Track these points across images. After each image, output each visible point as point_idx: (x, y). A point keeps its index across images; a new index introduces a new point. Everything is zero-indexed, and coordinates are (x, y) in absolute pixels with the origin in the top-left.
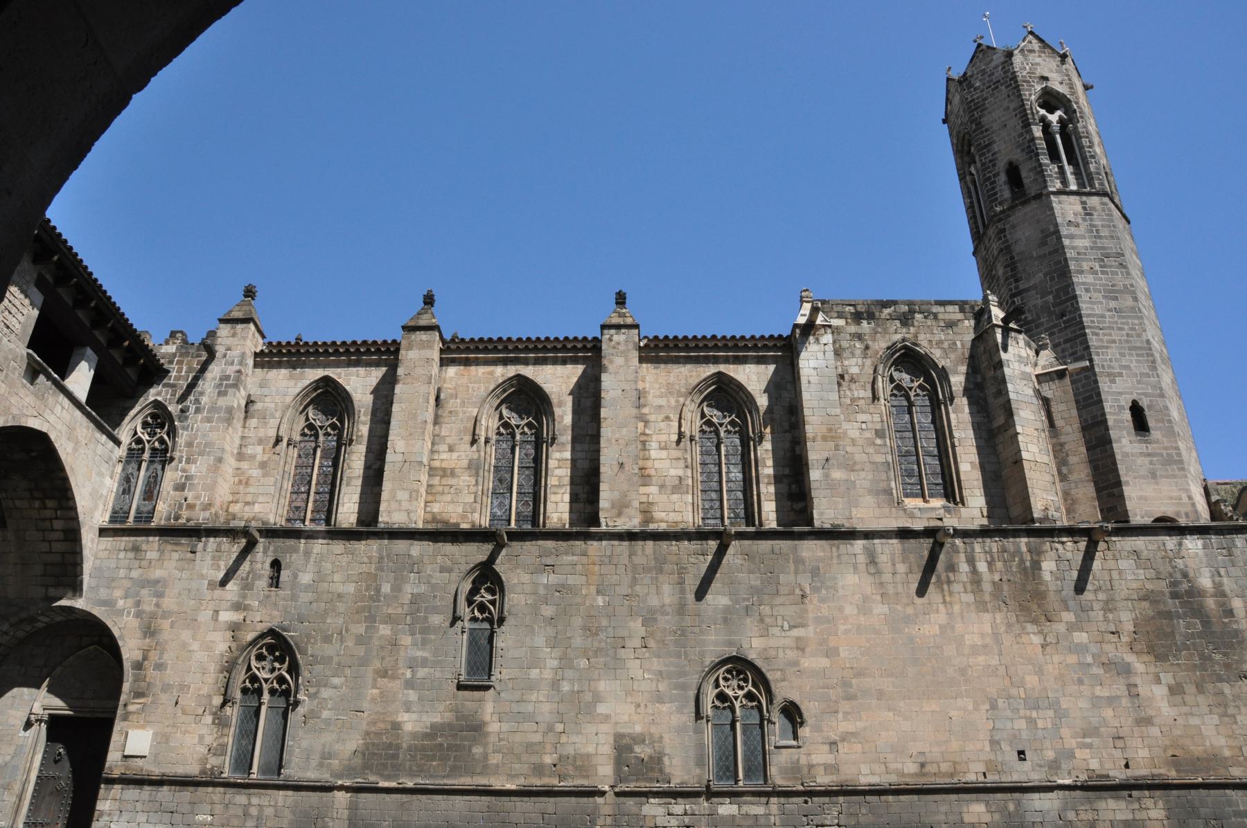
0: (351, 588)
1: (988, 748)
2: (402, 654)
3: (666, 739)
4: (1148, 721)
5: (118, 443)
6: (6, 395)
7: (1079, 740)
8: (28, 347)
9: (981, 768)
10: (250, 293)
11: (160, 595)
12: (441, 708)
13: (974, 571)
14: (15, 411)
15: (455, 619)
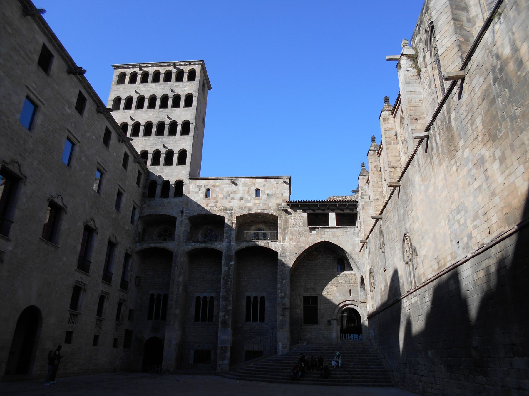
0: (374, 249)
1: (450, 247)
2: (380, 266)
3: (403, 276)
4: (493, 195)
5: (357, 227)
6: (306, 240)
7: (472, 225)
8: (308, 226)
9: (449, 258)
10: (363, 165)
11: (365, 266)
12: (384, 280)
13: (437, 144)
14: (311, 242)
15: (381, 249)
